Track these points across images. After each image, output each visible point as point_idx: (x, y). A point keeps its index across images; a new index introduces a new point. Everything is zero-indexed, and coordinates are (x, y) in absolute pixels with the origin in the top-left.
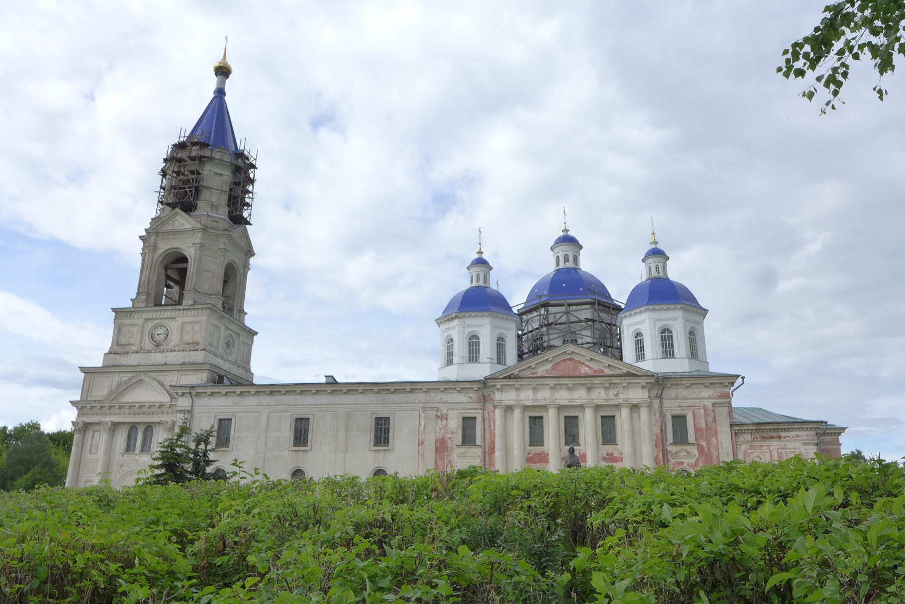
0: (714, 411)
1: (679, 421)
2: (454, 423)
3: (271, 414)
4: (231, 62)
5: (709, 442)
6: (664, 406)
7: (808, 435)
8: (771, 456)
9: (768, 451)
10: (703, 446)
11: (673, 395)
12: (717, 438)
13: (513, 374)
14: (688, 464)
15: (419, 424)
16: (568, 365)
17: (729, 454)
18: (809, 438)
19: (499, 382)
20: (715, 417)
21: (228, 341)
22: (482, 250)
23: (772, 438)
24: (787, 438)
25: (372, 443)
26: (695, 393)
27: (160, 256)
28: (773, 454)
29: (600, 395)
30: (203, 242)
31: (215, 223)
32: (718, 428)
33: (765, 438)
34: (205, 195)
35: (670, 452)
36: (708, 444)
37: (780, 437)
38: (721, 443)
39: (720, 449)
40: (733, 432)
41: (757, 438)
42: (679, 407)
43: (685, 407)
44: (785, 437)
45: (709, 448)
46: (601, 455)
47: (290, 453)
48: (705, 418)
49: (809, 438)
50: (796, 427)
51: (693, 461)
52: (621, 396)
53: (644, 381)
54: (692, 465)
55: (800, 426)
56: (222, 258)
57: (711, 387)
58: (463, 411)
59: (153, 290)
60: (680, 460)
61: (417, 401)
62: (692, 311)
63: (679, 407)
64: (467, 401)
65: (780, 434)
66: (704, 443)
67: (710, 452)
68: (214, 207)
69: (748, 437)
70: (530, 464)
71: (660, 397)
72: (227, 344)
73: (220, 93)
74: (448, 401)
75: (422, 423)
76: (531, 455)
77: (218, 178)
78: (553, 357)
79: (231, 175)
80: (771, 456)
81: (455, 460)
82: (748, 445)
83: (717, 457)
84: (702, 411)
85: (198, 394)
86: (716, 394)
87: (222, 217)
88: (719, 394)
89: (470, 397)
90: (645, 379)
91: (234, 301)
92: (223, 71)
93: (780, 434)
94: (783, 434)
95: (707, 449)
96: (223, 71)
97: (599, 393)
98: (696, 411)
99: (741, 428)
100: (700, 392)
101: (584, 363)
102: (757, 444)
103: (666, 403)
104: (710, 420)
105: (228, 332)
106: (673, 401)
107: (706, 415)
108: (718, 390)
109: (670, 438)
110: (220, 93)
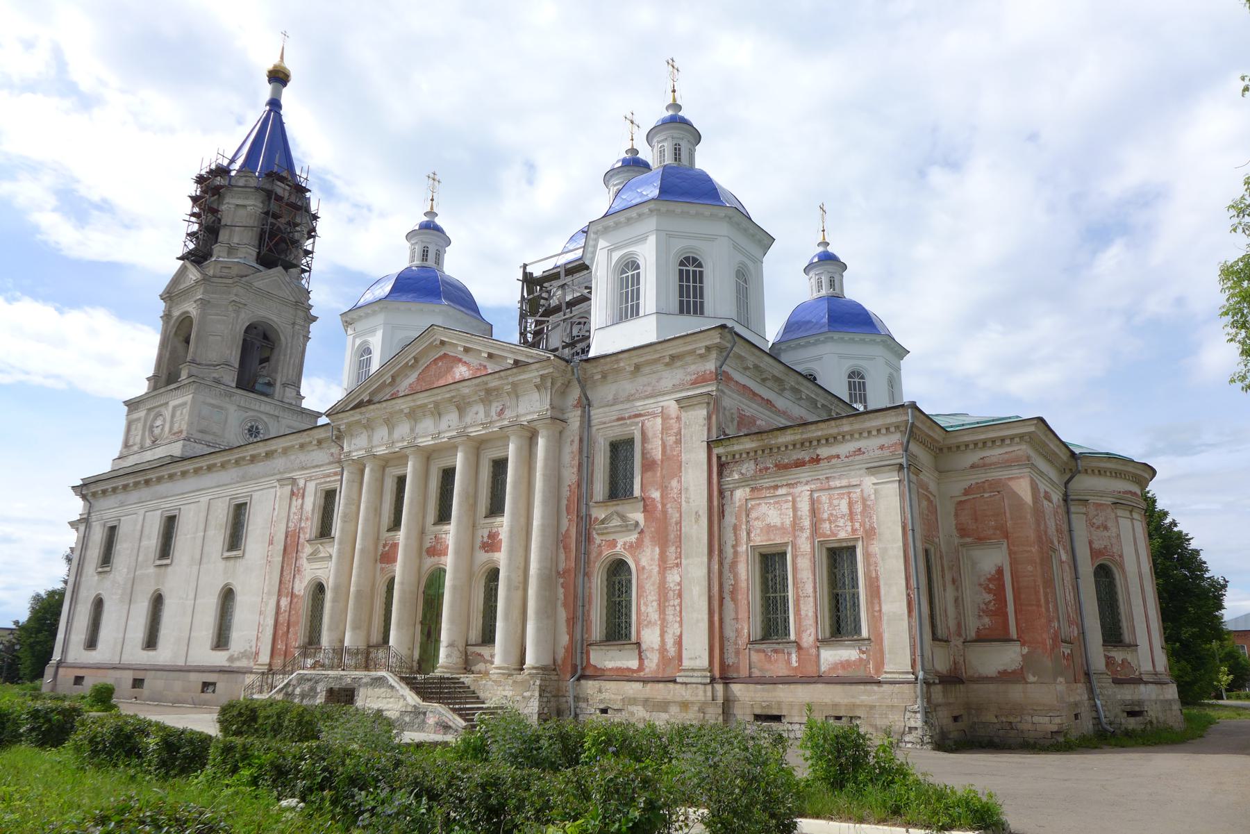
0: (678, 418)
1: (620, 450)
2: (311, 502)
3: (147, 514)
4: (289, 65)
5: (664, 490)
6: (594, 422)
7: (882, 447)
8: (795, 509)
9: (790, 498)
10: (653, 500)
11: (610, 397)
12: (679, 481)
13: (363, 400)
14: (625, 544)
15: (274, 509)
16: (441, 367)
17: (700, 513)
18: (886, 453)
19: (342, 419)
20: (679, 433)
21: (252, 427)
22: (435, 210)
23: (799, 464)
24: (834, 461)
25: (226, 547)
26: (649, 384)
27: (174, 324)
28: (799, 505)
29: (478, 421)
30: (206, 297)
31: (227, 271)
32: (684, 457)
33: (786, 467)
34: (224, 235)
35: (596, 519)
36: (662, 497)
37: (817, 460)
38: (687, 489)
39: (683, 503)
40: (714, 460)
41: (767, 469)
42: (618, 419)
43: (630, 418)
44: (829, 458)
45: (664, 505)
46: (480, 539)
47: (157, 570)
48: (662, 439)
49: (886, 453)
50: (846, 428)
51: (633, 537)
52: (509, 414)
53: (536, 374)
54: (631, 546)
55: (857, 426)
56: (233, 315)
57: (679, 364)
58: (323, 480)
59: (165, 372)
60: (611, 537)
61: (276, 471)
62: (713, 217)
63: (618, 419)
64: (328, 461)
65: (819, 451)
66: (656, 495)
67: (664, 512)
68: (231, 250)
69: (748, 468)
70: (383, 565)
71: (585, 404)
72: (249, 431)
73: (275, 104)
74: (308, 465)
75: (277, 507)
76: (387, 549)
77: (242, 212)
78: (416, 359)
79: (261, 205)
80: (795, 509)
81: (305, 565)
82: (748, 490)
83: (676, 524)
84: (659, 420)
85: (94, 494)
86: (688, 378)
87: (242, 261)
88: (694, 377)
89: (332, 454)
90: (537, 370)
91: (276, 373)
92: (279, 77)
93: (819, 451)
94: (824, 452)
95: (660, 506)
96: (279, 77)
97: (477, 414)
98: (648, 424)
99: (736, 448)
100: (659, 380)
101: (460, 360)
102: (766, 482)
103: (597, 414)
104: (671, 440)
105: (250, 413)
106: (607, 409)
107: (665, 429)
108: (693, 368)
109: (600, 488)
110: (275, 104)
